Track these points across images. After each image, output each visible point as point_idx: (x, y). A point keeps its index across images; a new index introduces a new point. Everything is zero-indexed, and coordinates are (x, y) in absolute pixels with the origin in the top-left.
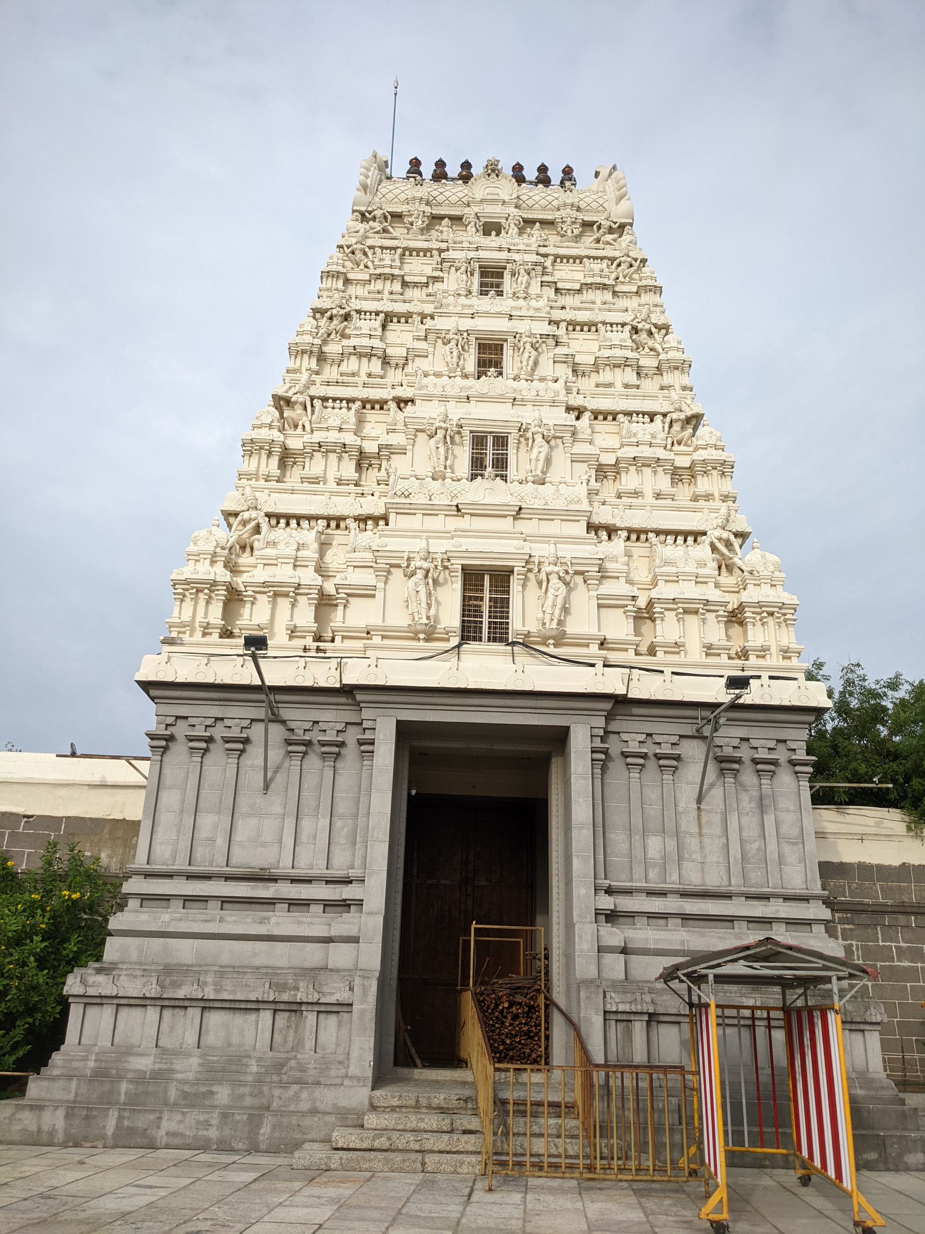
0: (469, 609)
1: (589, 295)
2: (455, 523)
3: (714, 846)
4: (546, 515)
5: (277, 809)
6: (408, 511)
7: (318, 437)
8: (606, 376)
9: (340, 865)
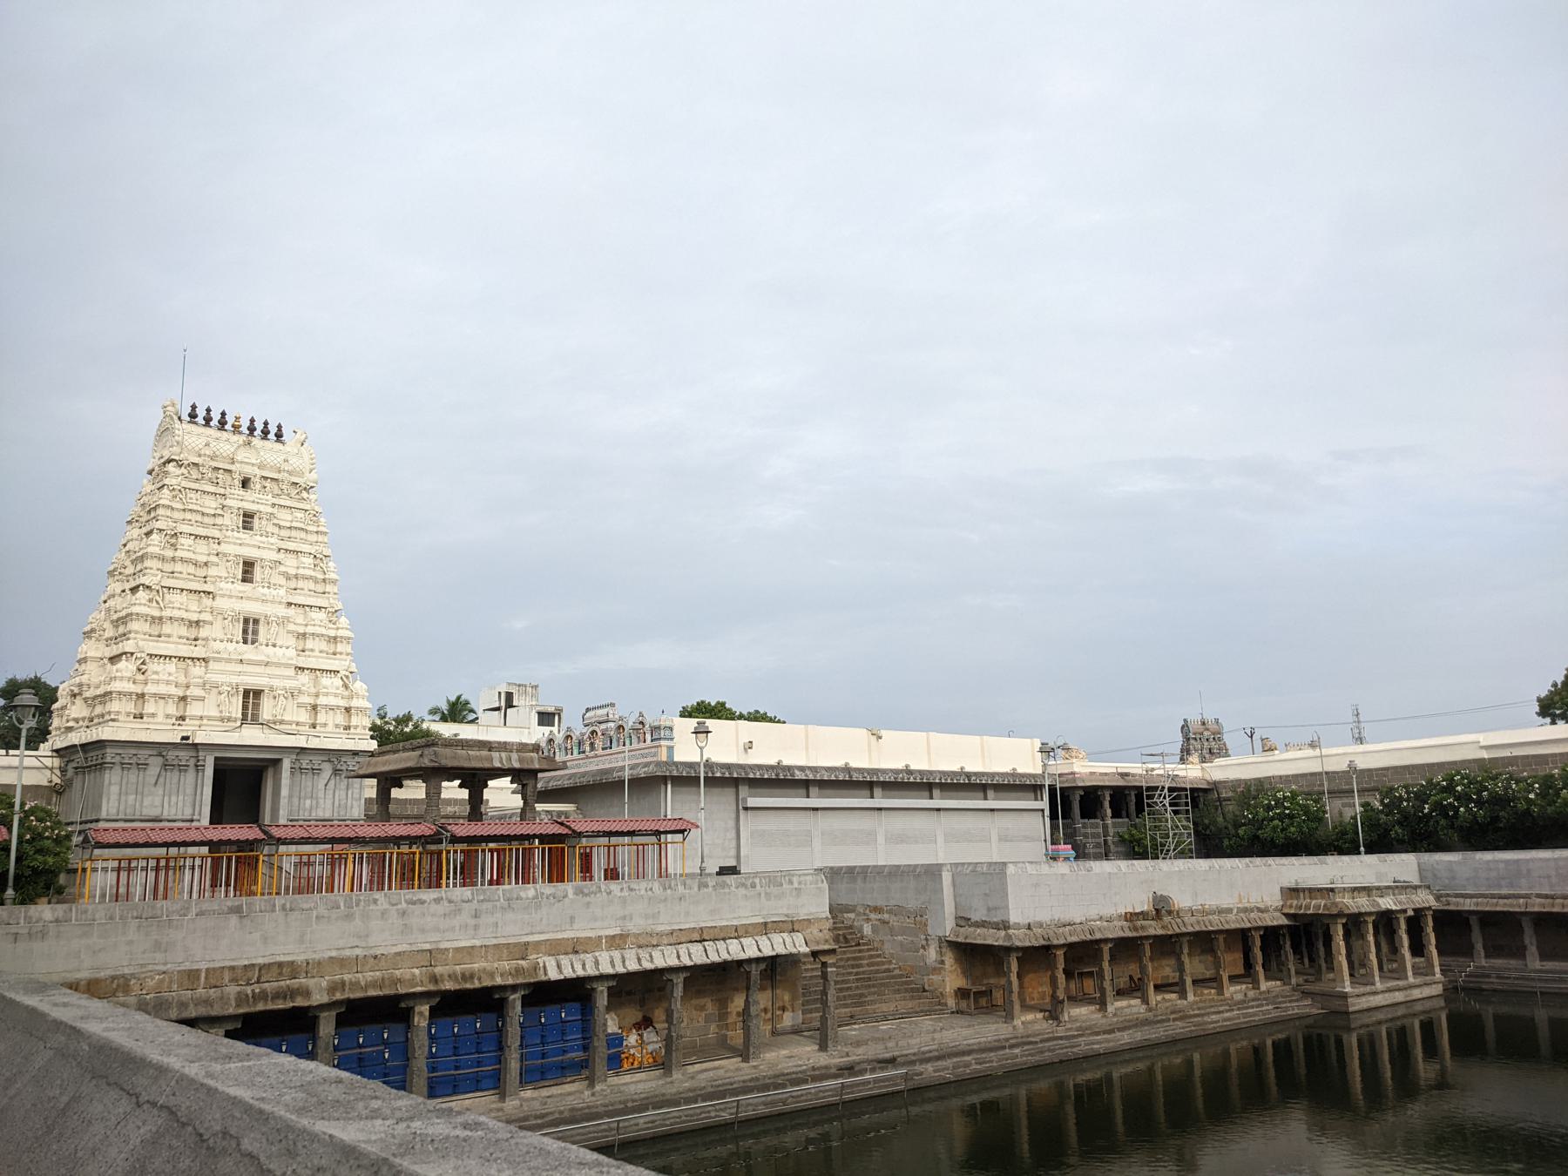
0: (245, 707)
1: (294, 533)
2: (240, 668)
3: (329, 802)
4: (278, 665)
7: (167, 613)
8: (301, 584)
9: (187, 814)
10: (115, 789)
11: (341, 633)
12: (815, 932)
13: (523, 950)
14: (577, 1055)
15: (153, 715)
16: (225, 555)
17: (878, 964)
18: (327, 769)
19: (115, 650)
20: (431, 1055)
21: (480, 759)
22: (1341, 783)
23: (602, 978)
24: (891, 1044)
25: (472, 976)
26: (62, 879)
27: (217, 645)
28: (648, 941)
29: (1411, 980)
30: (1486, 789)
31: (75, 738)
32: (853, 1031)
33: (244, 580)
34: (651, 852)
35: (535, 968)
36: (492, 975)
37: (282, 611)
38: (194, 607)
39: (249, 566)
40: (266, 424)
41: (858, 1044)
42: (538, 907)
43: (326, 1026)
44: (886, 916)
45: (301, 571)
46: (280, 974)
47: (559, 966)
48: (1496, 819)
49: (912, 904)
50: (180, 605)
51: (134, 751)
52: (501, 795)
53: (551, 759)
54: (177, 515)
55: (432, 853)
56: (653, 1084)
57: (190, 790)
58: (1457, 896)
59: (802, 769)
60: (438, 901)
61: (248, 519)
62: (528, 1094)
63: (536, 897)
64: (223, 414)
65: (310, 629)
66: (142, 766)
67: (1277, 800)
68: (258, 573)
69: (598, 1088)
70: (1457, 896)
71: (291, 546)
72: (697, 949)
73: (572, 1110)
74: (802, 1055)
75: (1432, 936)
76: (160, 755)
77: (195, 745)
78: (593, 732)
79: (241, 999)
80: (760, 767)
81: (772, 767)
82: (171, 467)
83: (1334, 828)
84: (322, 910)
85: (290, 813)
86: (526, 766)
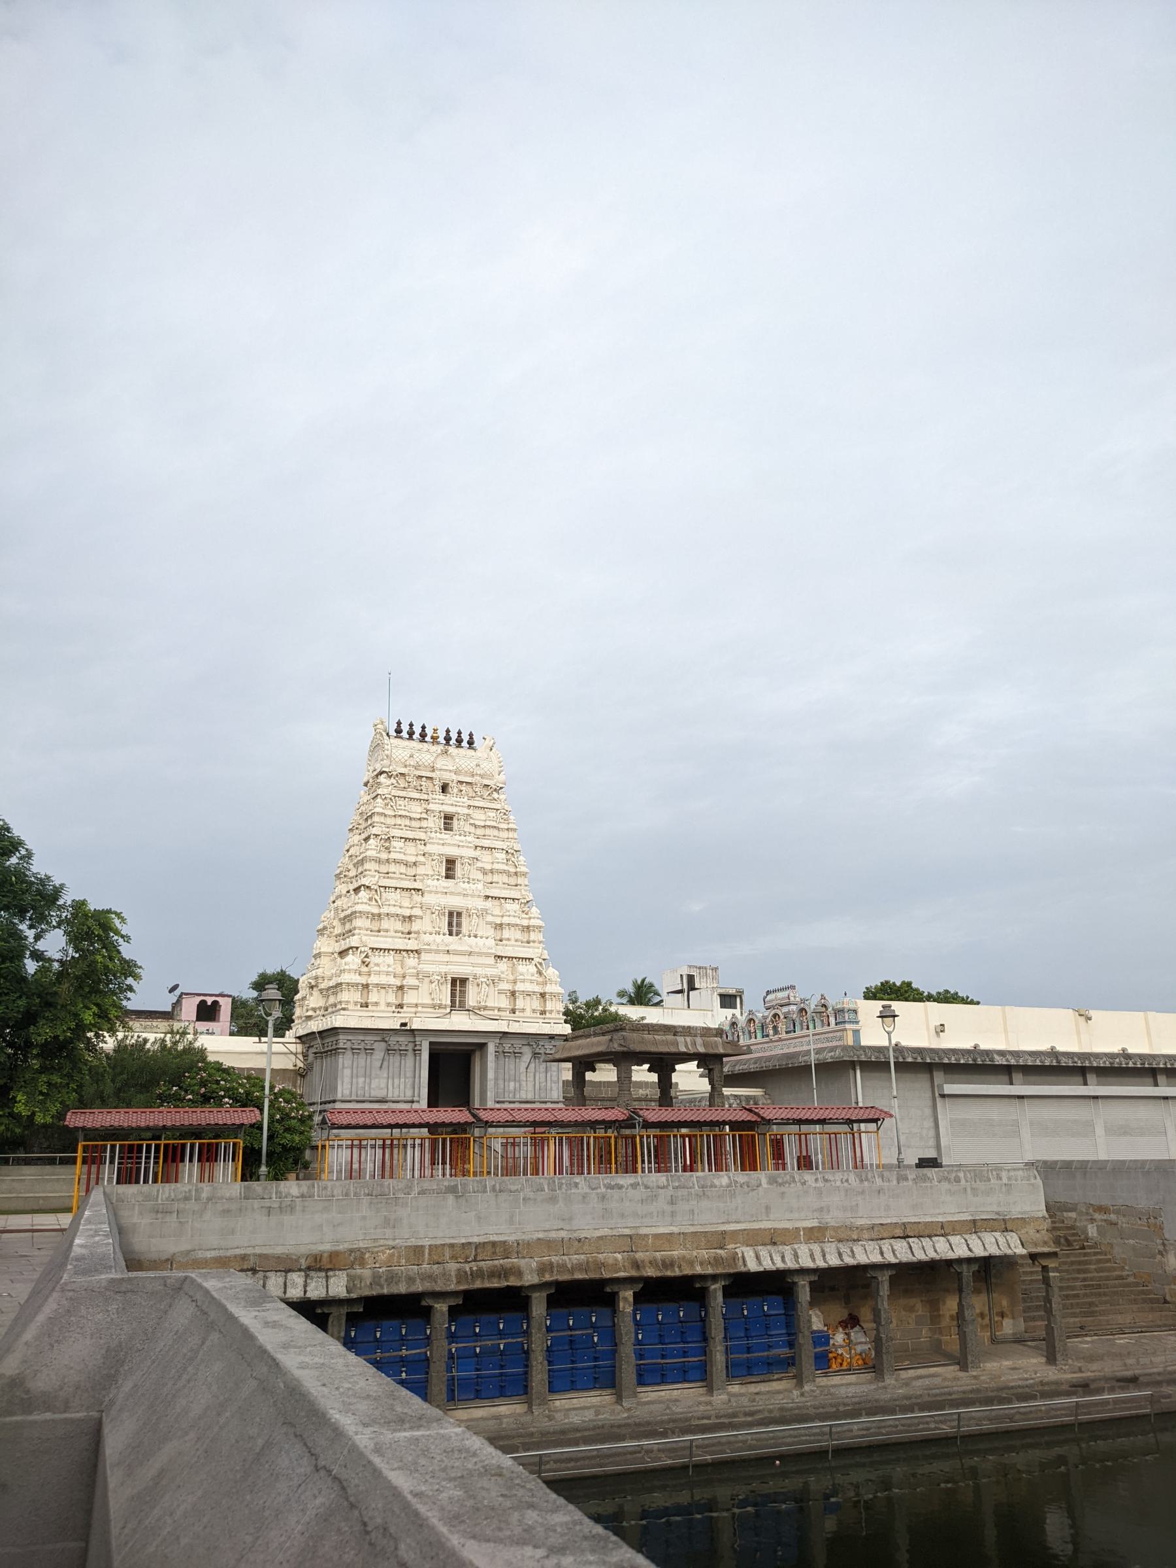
0: (453, 995)
1: (488, 831)
2: (446, 958)
3: (530, 1085)
4: (480, 954)
5: (385, 1075)
6: (429, 951)
7: (385, 910)
8: (496, 878)
9: (409, 1094)
10: (347, 1072)
11: (533, 922)
12: (1032, 1232)
13: (721, 1239)
14: (783, 1352)
15: (376, 1004)
16: (430, 855)
17: (1109, 1270)
18: (527, 1053)
19: (344, 945)
20: (638, 1342)
21: (667, 1043)
23: (803, 1271)
24: (1131, 1361)
25: (672, 1264)
26: (308, 1154)
27: (427, 938)
28: (848, 1235)
31: (315, 1026)
32: (1085, 1344)
33: (447, 877)
34: (845, 1142)
35: (734, 1257)
36: (691, 1263)
37: (481, 904)
38: (406, 903)
39: (450, 863)
40: (459, 733)
41: (1092, 1358)
42: (733, 1195)
43: (539, 1307)
44: (1113, 1217)
45: (496, 866)
46: (494, 1253)
47: (758, 1257)
49: (1143, 1202)
50: (396, 903)
51: (362, 1038)
52: (689, 1079)
53: (734, 1043)
54: (389, 821)
55: (626, 1137)
56: (865, 1388)
57: (409, 1074)
59: (1002, 1053)
60: (634, 1186)
61: (448, 818)
62: (735, 1389)
63: (729, 1186)
64: (424, 727)
65: (506, 920)
66: (369, 1051)
68: (459, 870)
69: (807, 1388)
71: (486, 843)
72: (900, 1246)
73: (781, 1409)
74: (1028, 1367)
76: (383, 1040)
77: (412, 1031)
78: (775, 1015)
79: (461, 1276)
80: (954, 1051)
81: (968, 1052)
82: (382, 778)
84: (528, 1193)
85: (497, 1094)
86: (711, 1051)
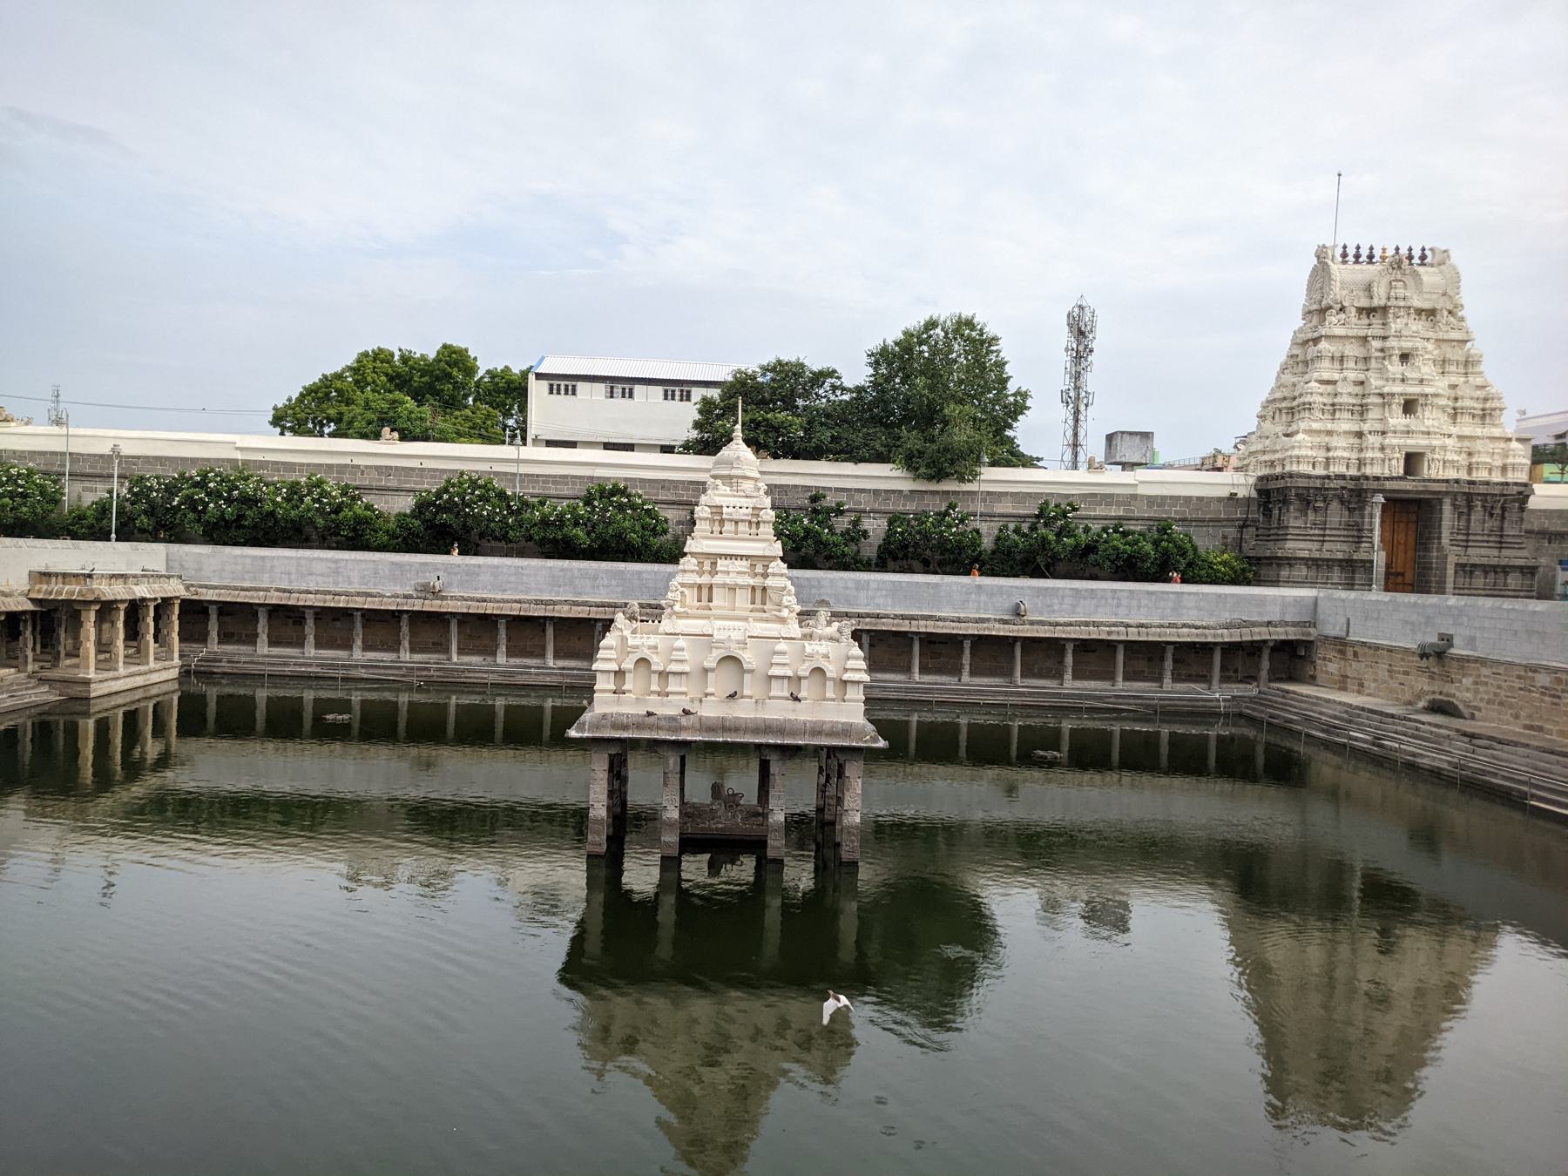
22: (91, 468)
29: (152, 664)
30: (237, 488)
48: (241, 517)
58: (201, 586)
67: (10, 478)
70: (201, 586)
75: (177, 623)
83: (70, 512)
